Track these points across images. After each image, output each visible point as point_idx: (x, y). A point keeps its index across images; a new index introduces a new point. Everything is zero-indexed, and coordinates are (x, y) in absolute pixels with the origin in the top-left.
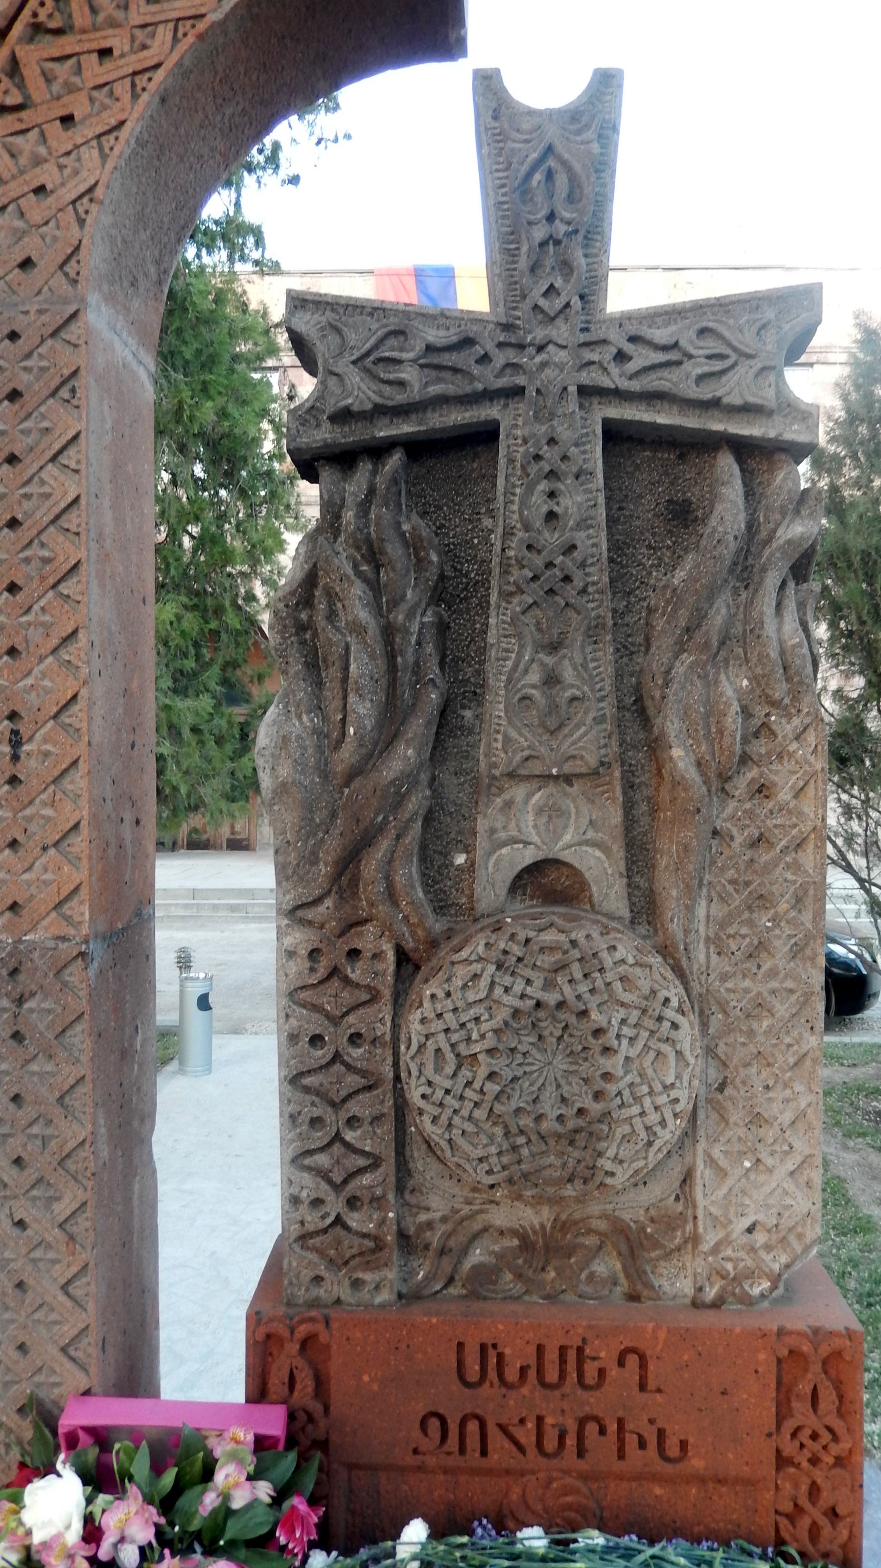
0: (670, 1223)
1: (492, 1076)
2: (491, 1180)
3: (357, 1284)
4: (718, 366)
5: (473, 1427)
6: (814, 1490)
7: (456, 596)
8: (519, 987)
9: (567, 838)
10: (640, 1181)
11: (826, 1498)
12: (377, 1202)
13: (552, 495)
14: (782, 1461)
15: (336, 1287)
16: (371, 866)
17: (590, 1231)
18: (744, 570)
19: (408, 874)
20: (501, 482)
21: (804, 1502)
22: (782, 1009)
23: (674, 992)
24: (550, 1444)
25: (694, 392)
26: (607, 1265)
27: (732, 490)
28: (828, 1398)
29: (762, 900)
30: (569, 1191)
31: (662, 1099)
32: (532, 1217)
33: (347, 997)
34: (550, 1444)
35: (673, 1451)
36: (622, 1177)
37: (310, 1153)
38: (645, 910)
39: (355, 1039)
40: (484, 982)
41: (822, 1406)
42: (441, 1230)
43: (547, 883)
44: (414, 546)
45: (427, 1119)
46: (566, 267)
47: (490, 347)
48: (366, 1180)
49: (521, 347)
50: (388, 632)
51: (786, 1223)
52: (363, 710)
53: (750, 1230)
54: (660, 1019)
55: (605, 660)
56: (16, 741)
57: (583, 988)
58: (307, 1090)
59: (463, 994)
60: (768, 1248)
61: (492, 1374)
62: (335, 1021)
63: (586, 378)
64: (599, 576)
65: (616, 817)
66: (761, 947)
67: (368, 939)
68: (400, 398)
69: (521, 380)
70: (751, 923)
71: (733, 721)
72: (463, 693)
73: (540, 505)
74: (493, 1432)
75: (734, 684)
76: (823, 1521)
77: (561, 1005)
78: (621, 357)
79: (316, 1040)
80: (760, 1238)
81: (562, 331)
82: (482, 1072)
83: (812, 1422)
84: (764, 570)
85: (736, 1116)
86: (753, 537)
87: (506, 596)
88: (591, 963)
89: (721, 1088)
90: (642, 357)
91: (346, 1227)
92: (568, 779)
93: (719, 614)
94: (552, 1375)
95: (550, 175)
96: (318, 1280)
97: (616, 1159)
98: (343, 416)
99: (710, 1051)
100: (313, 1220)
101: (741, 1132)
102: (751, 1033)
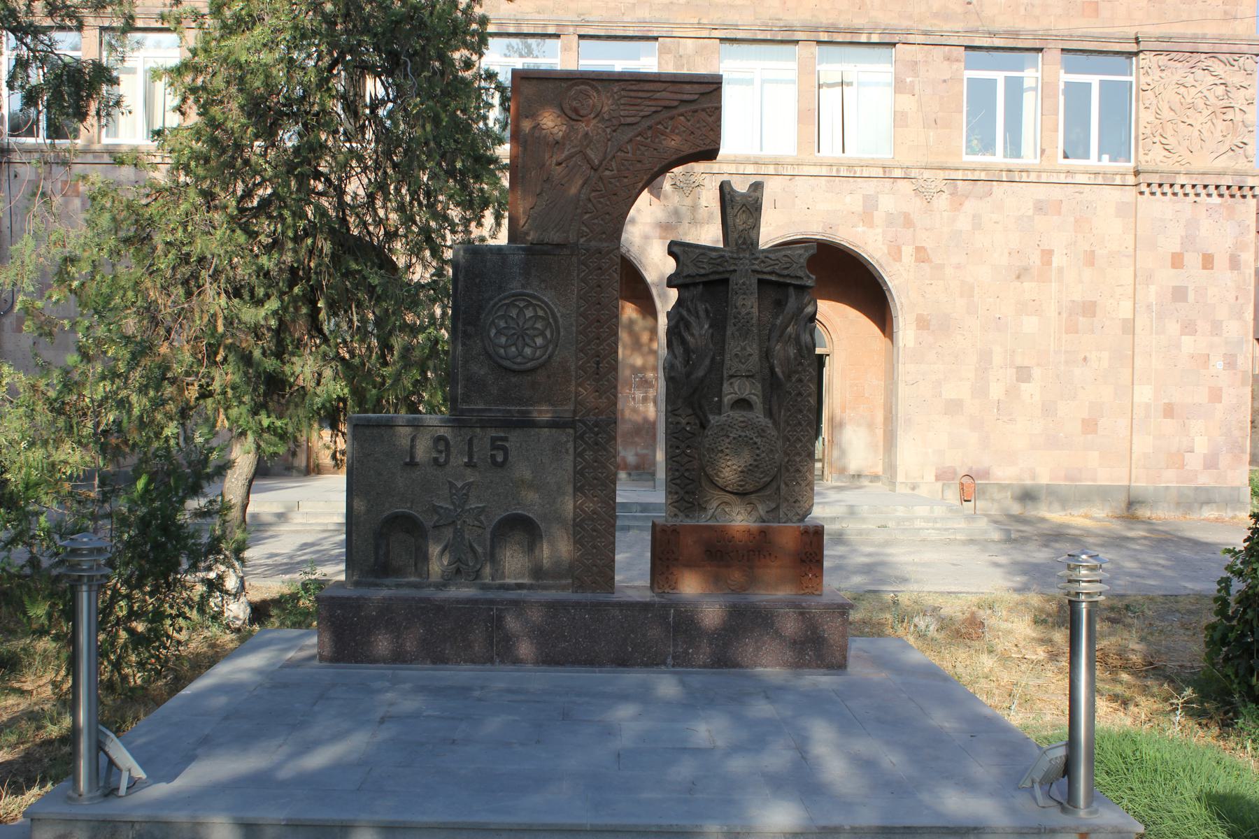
39: (688, 447)
56: (598, 363)
98: (688, 276)
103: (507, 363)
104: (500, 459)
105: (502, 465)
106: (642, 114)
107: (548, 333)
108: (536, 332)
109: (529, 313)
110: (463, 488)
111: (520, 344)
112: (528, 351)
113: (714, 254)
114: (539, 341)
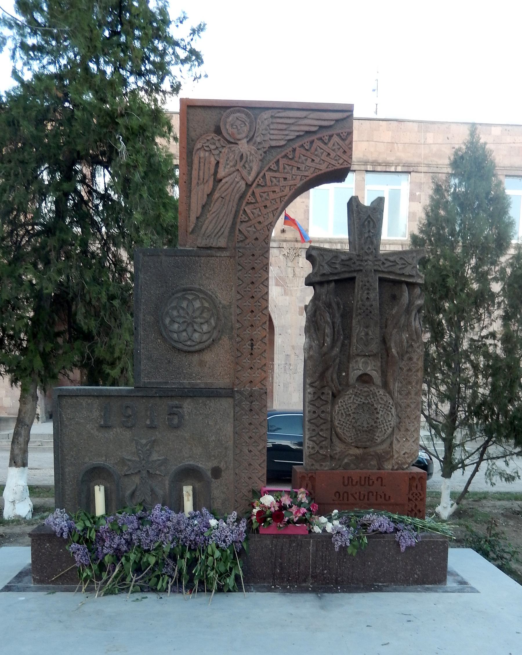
0: (387, 453)
1: (354, 418)
2: (351, 441)
3: (321, 465)
4: (404, 266)
5: (345, 494)
6: (416, 506)
7: (346, 315)
8: (359, 399)
9: (369, 369)
10: (383, 442)
11: (418, 508)
12: (326, 448)
13: (368, 294)
14: (410, 500)
15: (317, 466)
16: (328, 374)
17: (371, 455)
18: (408, 311)
19: (335, 376)
20: (356, 291)
21: (414, 509)
22: (413, 406)
23: (391, 401)
24: (362, 498)
25: (399, 272)
26: (374, 463)
27: (406, 294)
28: (419, 487)
29: (410, 383)
30: (368, 444)
31: (388, 424)
32: (358, 452)
33: (321, 402)
34: (362, 498)
35: (387, 497)
36: (379, 440)
37: (312, 437)
38: (385, 385)
39: (323, 412)
40: (352, 399)
41: (418, 488)
42: (339, 454)
43: (365, 379)
44: (338, 304)
45: (338, 429)
46: (372, 243)
47: (355, 260)
48: (324, 443)
49: (362, 261)
50: (333, 323)
51: (412, 452)
52: (328, 340)
53: (404, 454)
54: (388, 407)
55: (378, 330)
56: (252, 345)
57: (373, 400)
58: (311, 423)
59: (348, 401)
60: (408, 458)
61: (350, 483)
62: (318, 408)
63: (375, 268)
64: (377, 312)
65: (379, 364)
66: (409, 393)
67: (326, 390)
68: (336, 271)
69: (362, 268)
70: (407, 388)
71: (405, 344)
72: (348, 337)
73: (365, 296)
74: (350, 496)
75: (405, 336)
76: (417, 512)
77: (369, 403)
78: (383, 263)
79: (314, 412)
80: (406, 456)
81: (371, 257)
82: (352, 417)
83: (416, 492)
84: (412, 311)
85: (402, 429)
86: (411, 303)
87: (357, 316)
88: (374, 395)
89: (399, 423)
90: (388, 264)
91: (319, 453)
92: (369, 356)
93: (403, 320)
94: (363, 483)
95: (369, 222)
96: (313, 465)
97: (378, 437)
98: (323, 275)
99: (397, 415)
100: (312, 452)
101: (403, 433)
102: (406, 412)
103: (180, 346)
104: (176, 421)
105: (177, 427)
106: (288, 138)
107: (213, 321)
108: (202, 321)
109: (197, 304)
110: (146, 445)
111: (190, 329)
112: (196, 336)
113: (343, 257)
114: (205, 328)
